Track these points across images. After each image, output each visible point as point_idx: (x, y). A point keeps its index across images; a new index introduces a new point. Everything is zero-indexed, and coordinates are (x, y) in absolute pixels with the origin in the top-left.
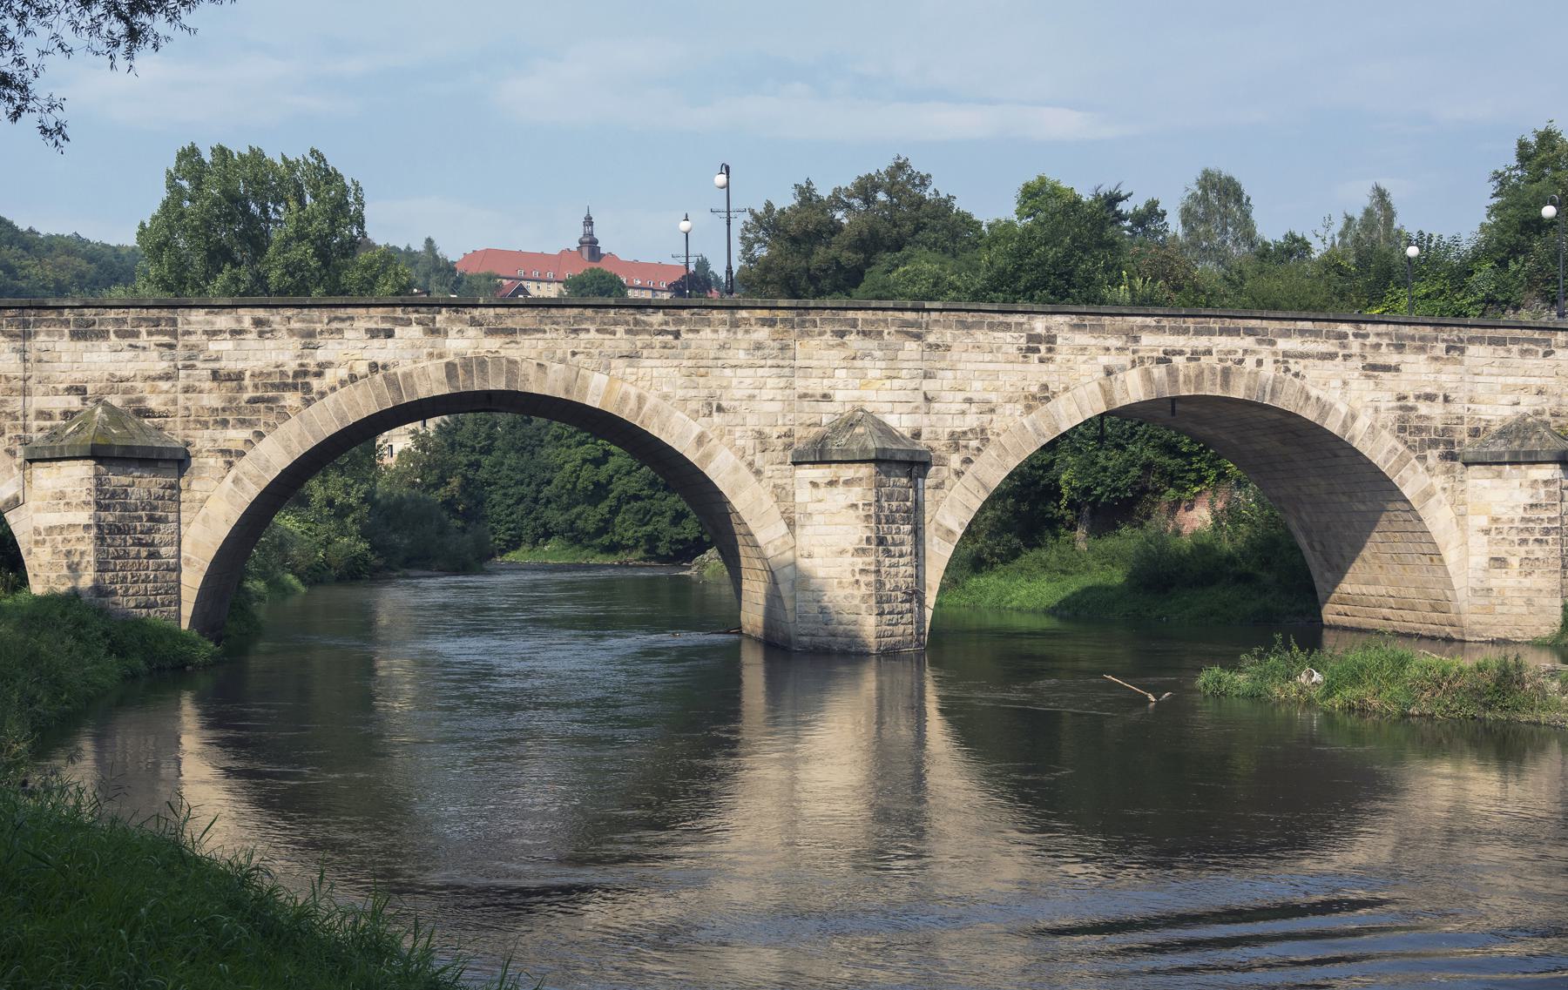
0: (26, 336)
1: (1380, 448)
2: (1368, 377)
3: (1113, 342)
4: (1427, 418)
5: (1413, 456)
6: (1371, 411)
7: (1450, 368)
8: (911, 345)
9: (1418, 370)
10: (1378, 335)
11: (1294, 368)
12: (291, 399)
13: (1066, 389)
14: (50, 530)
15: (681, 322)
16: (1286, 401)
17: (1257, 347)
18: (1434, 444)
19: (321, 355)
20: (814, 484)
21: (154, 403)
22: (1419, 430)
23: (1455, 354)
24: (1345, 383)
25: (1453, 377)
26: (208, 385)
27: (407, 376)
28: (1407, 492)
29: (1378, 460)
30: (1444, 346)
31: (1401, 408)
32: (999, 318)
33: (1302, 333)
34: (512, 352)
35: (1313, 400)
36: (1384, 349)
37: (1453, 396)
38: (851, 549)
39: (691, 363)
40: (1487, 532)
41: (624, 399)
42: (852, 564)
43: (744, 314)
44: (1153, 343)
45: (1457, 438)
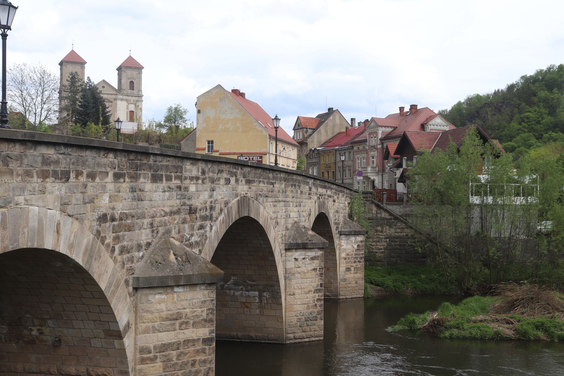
0: (135, 178)
14: (164, 347)
20: (296, 259)
27: (231, 207)
38: (313, 290)
39: (274, 199)
40: (345, 259)
42: (314, 297)
44: (321, 190)
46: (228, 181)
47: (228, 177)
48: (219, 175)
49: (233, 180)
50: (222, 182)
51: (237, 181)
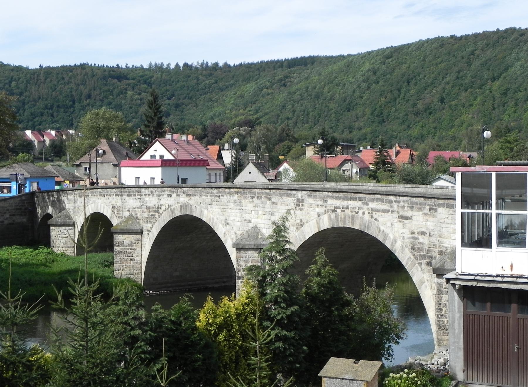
0: (122, 195)
1: (404, 257)
2: (400, 222)
3: (320, 203)
4: (422, 244)
5: (417, 262)
6: (401, 238)
7: (431, 219)
8: (268, 202)
9: (419, 220)
10: (404, 201)
11: (375, 216)
12: (157, 215)
13: (307, 222)
15: (220, 193)
16: (373, 232)
17: (362, 206)
18: (424, 257)
19: (161, 202)
21: (139, 216)
22: (419, 249)
23: (433, 212)
24: (392, 224)
25: (432, 224)
26: (145, 210)
27: (174, 209)
28: (415, 279)
29: (404, 262)
30: (428, 207)
31: (413, 238)
32: (289, 192)
33: (377, 200)
34: (191, 203)
35: (381, 232)
36: (406, 207)
37: (432, 233)
39: (222, 207)
41: (210, 219)
43: (232, 190)
44: (332, 203)
45: (434, 255)
46: (170, 196)
47: (170, 193)
48: (163, 193)
49: (174, 195)
50: (166, 196)
51: (177, 195)
